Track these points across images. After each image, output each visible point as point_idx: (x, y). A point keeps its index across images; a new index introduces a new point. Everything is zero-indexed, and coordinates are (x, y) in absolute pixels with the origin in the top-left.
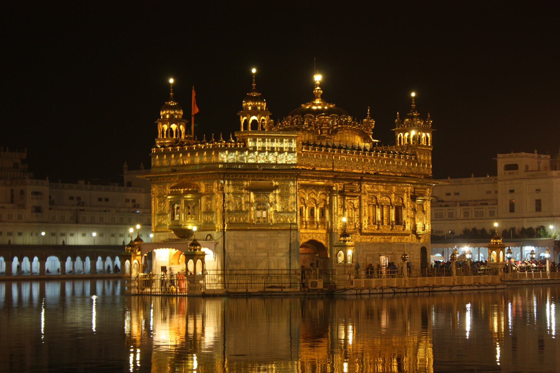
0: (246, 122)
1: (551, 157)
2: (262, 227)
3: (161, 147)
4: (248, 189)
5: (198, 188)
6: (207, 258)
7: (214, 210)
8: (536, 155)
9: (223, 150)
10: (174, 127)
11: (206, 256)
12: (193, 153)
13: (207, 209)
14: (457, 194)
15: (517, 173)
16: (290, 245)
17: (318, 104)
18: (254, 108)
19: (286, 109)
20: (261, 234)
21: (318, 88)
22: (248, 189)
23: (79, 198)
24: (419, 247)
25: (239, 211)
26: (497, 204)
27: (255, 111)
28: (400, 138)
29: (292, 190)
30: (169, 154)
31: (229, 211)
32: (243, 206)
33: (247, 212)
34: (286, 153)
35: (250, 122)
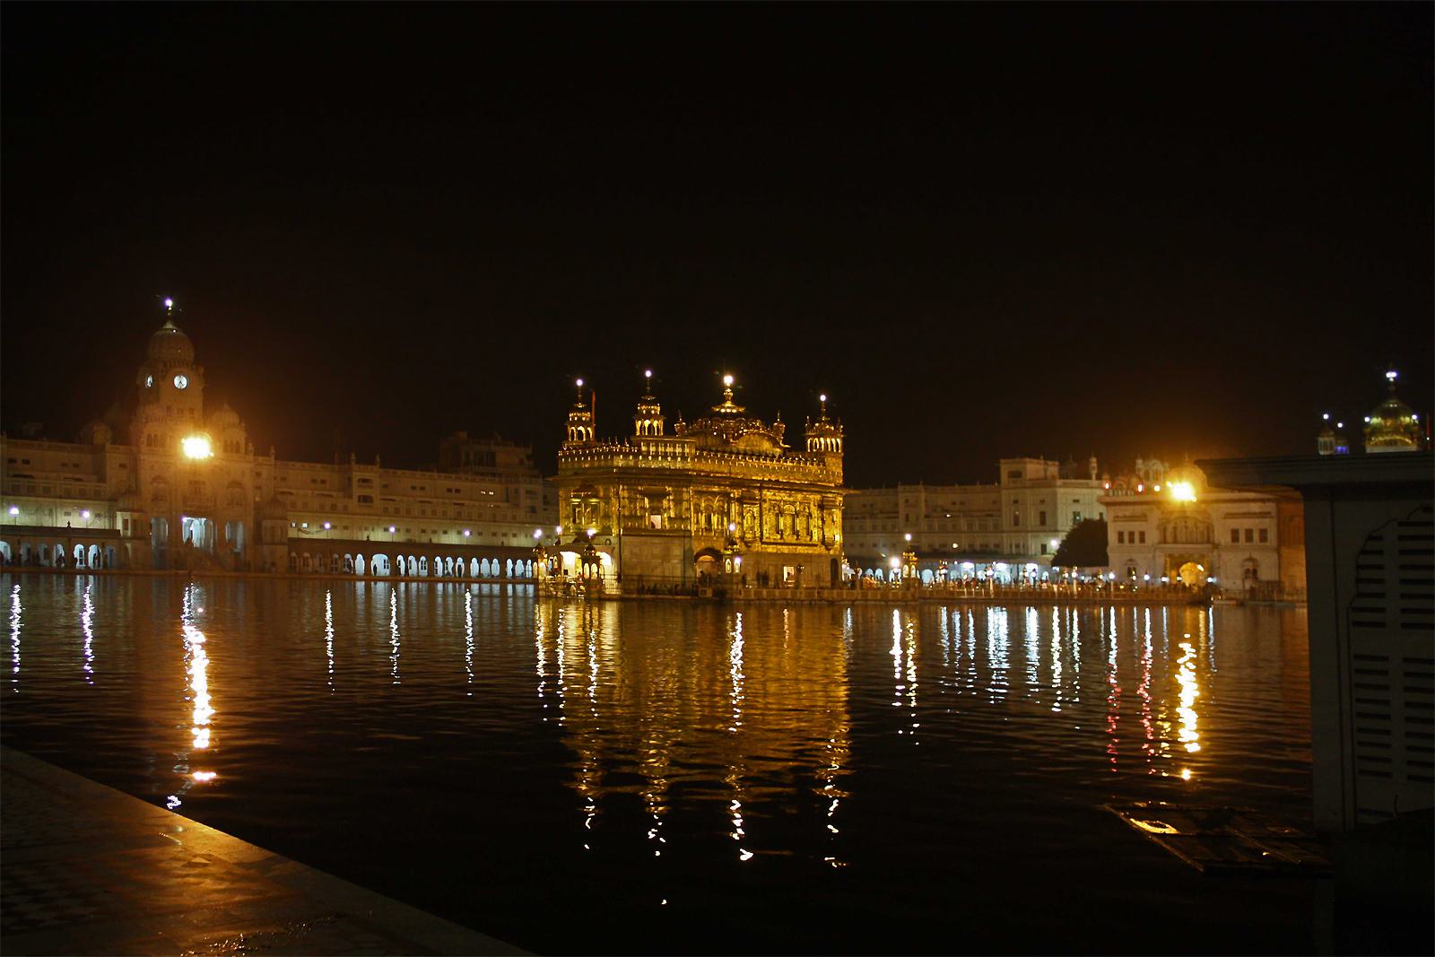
0: (642, 427)
1: (1061, 464)
2: (660, 534)
4: (641, 493)
5: (598, 492)
6: (602, 562)
8: (1042, 461)
9: (618, 454)
17: (728, 407)
18: (649, 411)
21: (729, 390)
22: (641, 493)
24: (830, 559)
25: (633, 517)
27: (649, 416)
28: (811, 444)
29: (685, 496)
31: (624, 516)
33: (642, 517)
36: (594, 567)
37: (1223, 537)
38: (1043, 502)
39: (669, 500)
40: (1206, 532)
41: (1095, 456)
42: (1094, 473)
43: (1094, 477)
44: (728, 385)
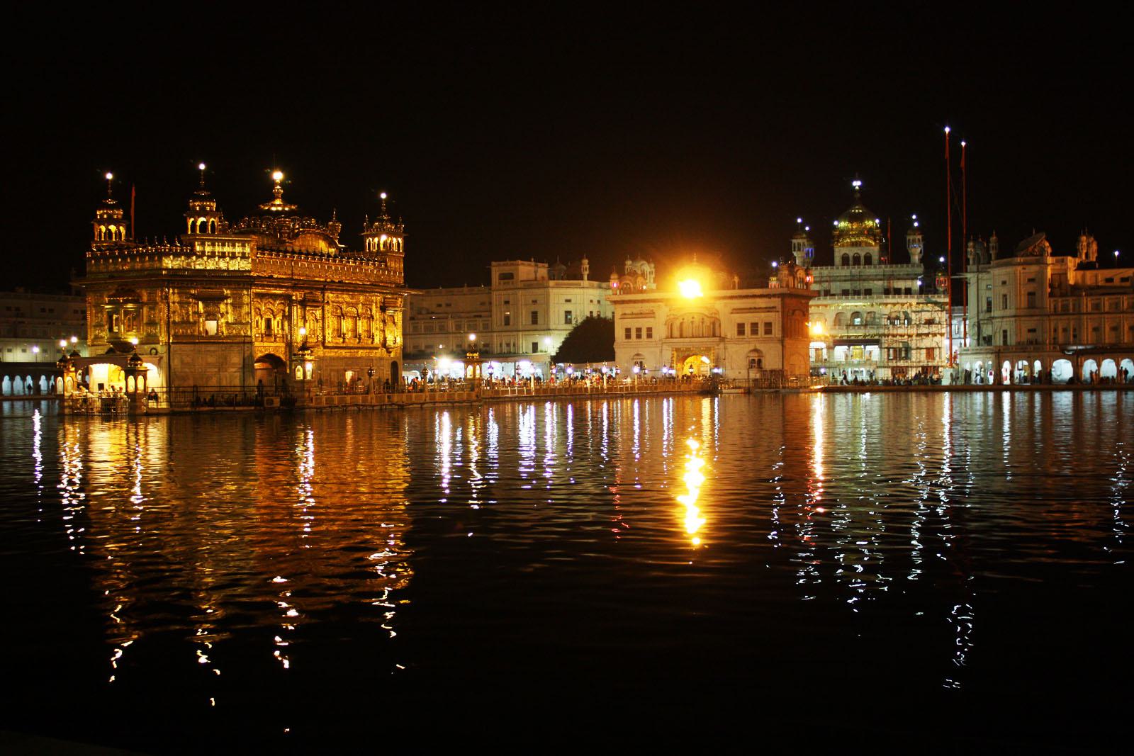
0: (194, 224)
1: (550, 266)
2: (216, 340)
3: (98, 250)
4: (193, 296)
5: (140, 296)
6: (149, 374)
7: (157, 321)
8: (533, 264)
9: (167, 255)
10: (113, 228)
11: (148, 372)
12: (133, 257)
13: (150, 320)
14: (448, 305)
15: (513, 283)
16: (244, 359)
17: (277, 205)
18: (203, 208)
19: (242, 211)
20: (212, 348)
21: (278, 187)
22: (193, 296)
23: (18, 309)
24: (390, 362)
25: (185, 322)
26: (491, 316)
27: (203, 212)
28: (369, 244)
29: (246, 300)
30: (106, 259)
31: (174, 322)
32: (191, 317)
33: (195, 323)
34: (239, 259)
35: (198, 224)
36: (140, 379)
37: (729, 330)
38: (535, 302)
39: (227, 304)
40: (1035, 318)
41: (587, 258)
42: (586, 273)
43: (586, 277)
44: (278, 181)
